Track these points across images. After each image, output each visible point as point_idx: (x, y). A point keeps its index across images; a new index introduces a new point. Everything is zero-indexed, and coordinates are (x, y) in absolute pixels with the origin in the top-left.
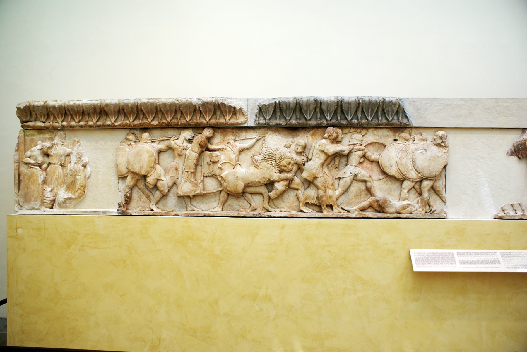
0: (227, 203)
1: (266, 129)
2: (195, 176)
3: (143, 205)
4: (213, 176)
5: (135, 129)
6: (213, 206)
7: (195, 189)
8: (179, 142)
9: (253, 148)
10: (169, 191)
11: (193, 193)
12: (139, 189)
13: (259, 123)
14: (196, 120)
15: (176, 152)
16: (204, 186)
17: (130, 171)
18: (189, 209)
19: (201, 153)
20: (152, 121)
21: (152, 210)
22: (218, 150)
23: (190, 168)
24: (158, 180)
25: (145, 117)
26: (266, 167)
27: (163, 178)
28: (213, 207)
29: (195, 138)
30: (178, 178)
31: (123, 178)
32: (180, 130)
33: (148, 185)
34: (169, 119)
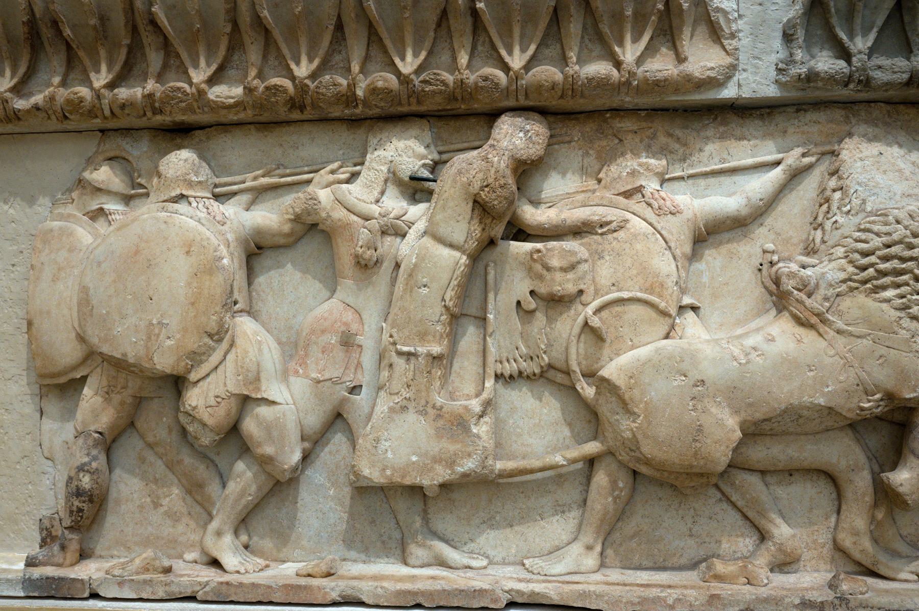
0: (630, 527)
1: (838, 114)
2: (445, 378)
3: (167, 530)
4: (551, 376)
5: (126, 131)
6: (554, 552)
7: (452, 447)
8: (356, 192)
9: (769, 221)
10: (306, 457)
11: (442, 474)
12: (150, 446)
13: (812, 77)
14: (453, 67)
15: (345, 252)
16: (498, 429)
17: (91, 355)
18: (418, 552)
19: (483, 252)
20: (212, 81)
21: (215, 563)
22: (579, 231)
23: (423, 336)
24: (245, 401)
25: (173, 64)
26: (867, 320)
27: (273, 390)
28: (548, 546)
29: (448, 173)
30: (355, 389)
31: (59, 387)
32: (361, 133)
33: (190, 429)
34: (302, 70)
